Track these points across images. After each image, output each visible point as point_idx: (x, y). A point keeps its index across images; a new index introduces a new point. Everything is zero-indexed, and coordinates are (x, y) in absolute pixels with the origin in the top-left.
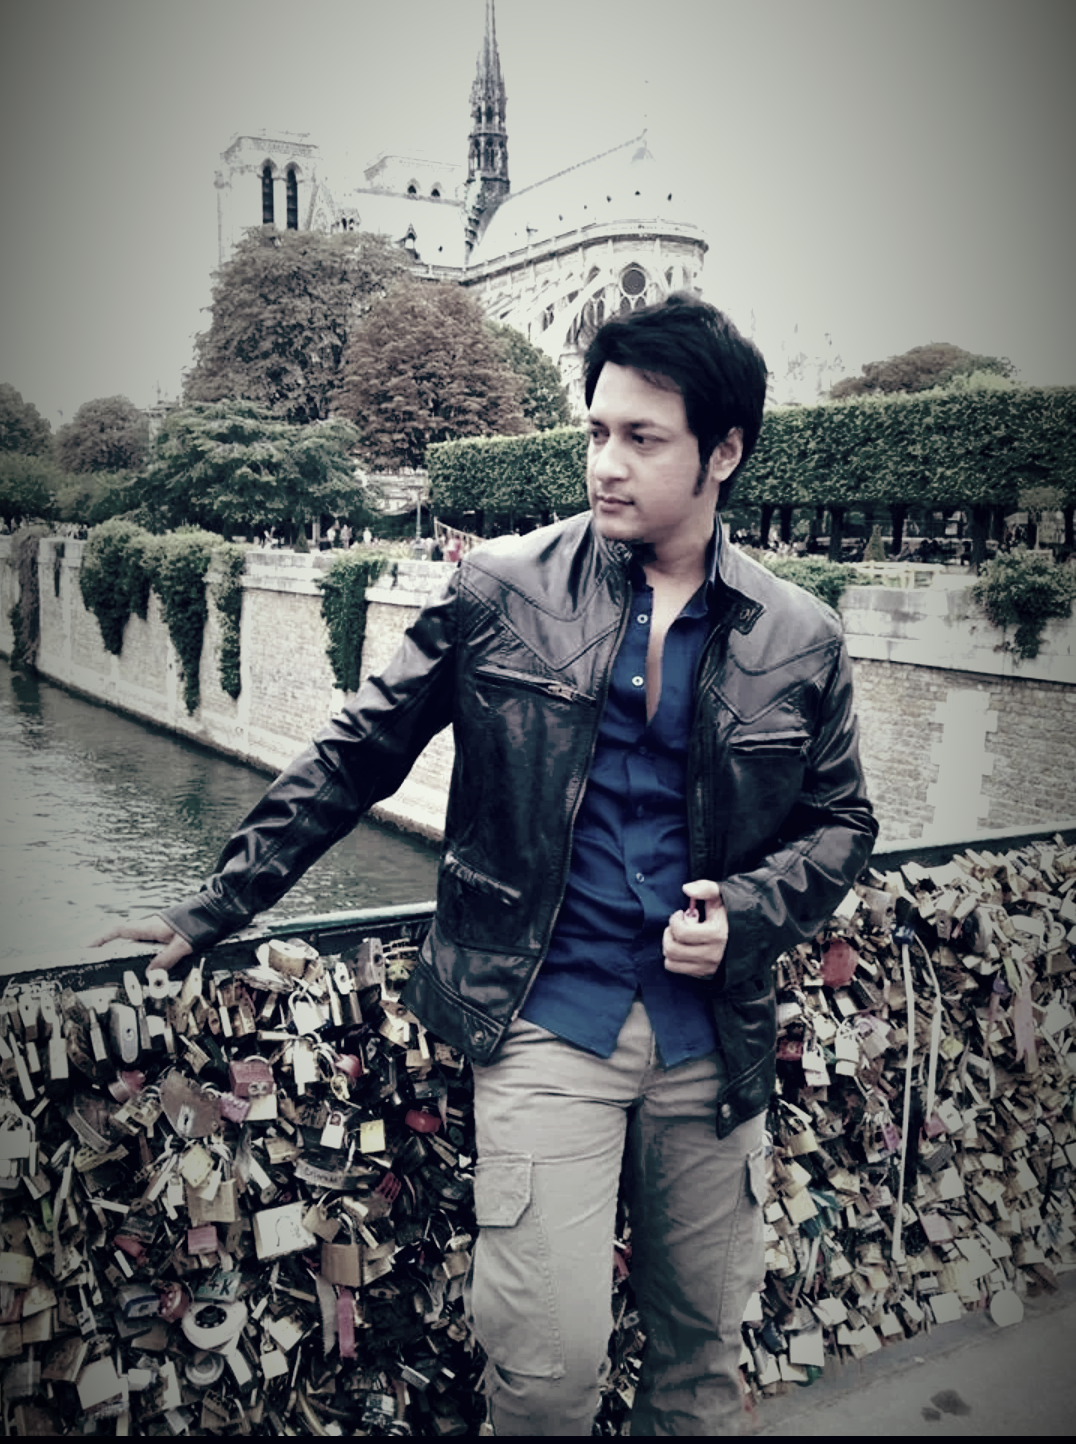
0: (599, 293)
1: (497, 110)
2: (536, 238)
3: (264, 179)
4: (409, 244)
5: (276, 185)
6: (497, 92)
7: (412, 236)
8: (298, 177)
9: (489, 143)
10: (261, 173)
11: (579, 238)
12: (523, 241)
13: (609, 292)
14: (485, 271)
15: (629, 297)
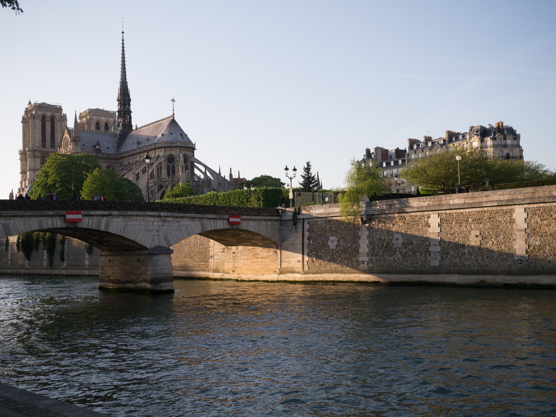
0: (160, 163)
1: (127, 103)
2: (141, 146)
3: (42, 121)
4: (97, 147)
5: (47, 123)
6: (127, 98)
7: (98, 144)
8: (55, 120)
9: (124, 114)
10: (41, 119)
11: (153, 147)
12: (135, 147)
13: (163, 164)
14: (124, 155)
15: (170, 164)
